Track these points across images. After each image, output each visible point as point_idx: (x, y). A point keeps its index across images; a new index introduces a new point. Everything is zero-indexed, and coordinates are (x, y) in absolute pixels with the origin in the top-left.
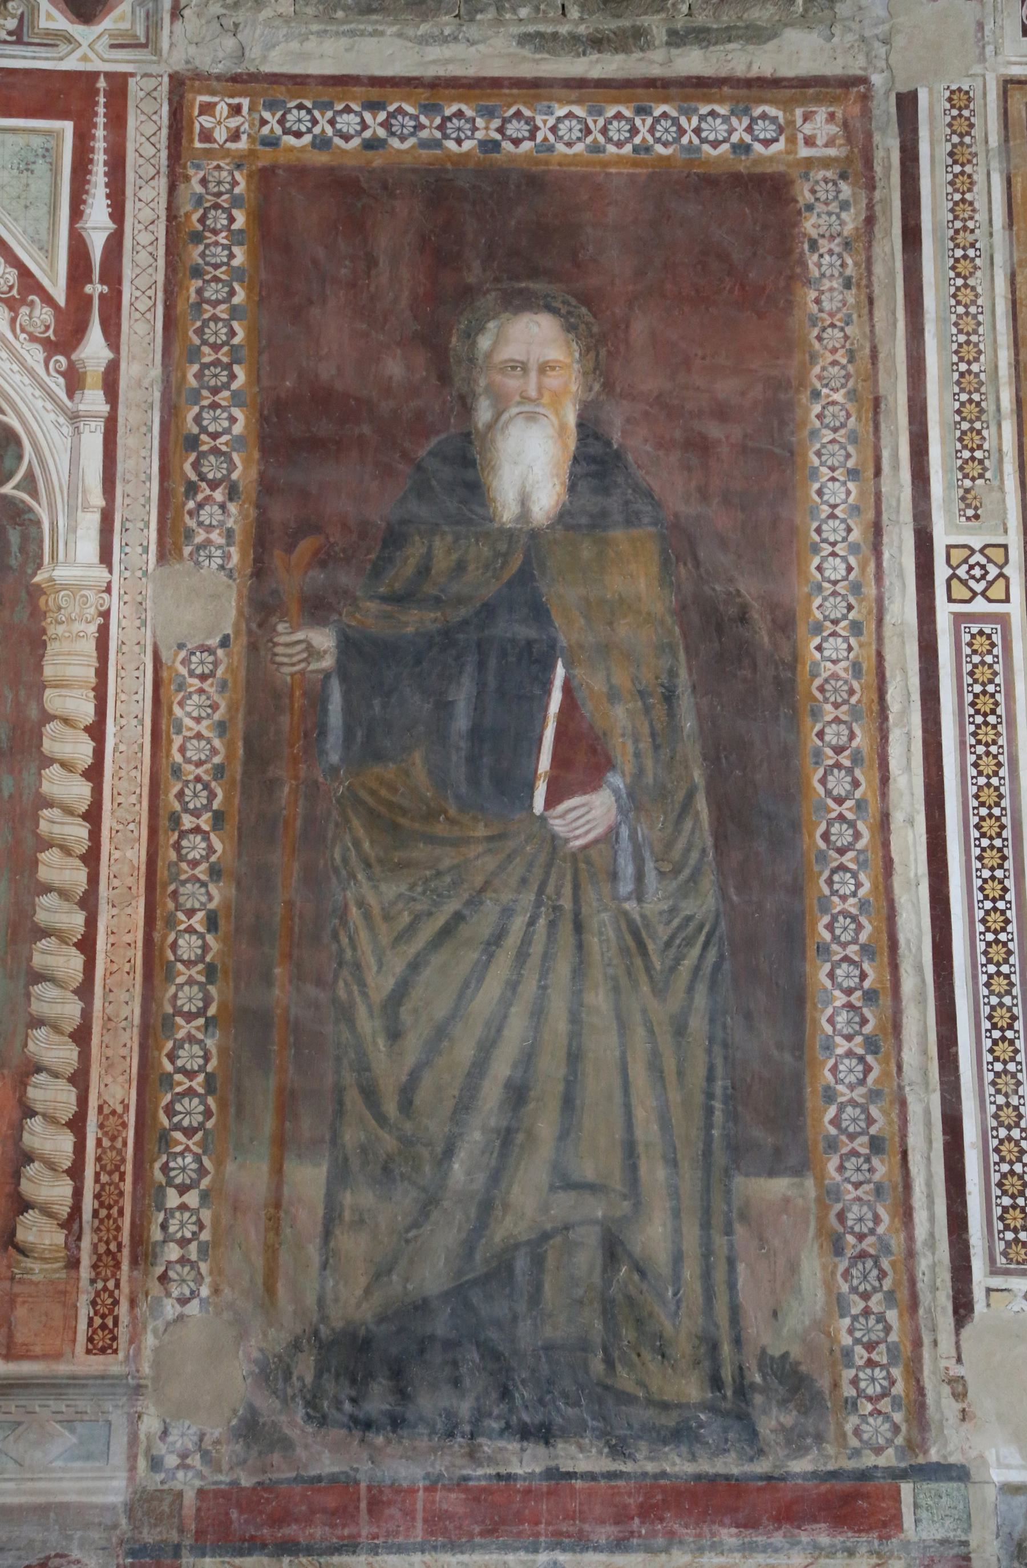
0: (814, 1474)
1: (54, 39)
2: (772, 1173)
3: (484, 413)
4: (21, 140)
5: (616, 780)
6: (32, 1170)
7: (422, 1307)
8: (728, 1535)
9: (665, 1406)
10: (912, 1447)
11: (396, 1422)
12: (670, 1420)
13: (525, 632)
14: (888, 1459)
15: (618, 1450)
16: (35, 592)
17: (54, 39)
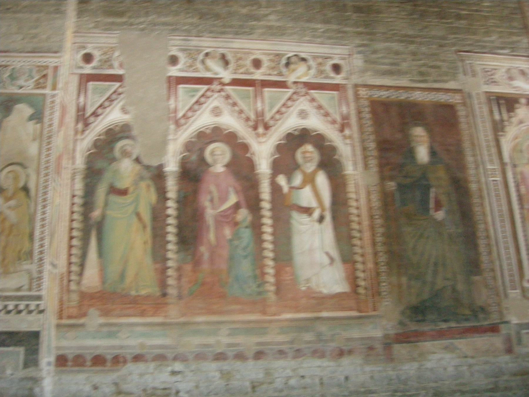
0: (488, 325)
1: (332, 78)
2: (476, 275)
3: (413, 144)
4: (330, 95)
5: (444, 209)
6: (359, 280)
7: (424, 301)
8: (477, 335)
9: (464, 315)
10: (501, 319)
11: (423, 321)
12: (464, 317)
13: (426, 183)
14: (499, 321)
15: (458, 322)
16: (345, 175)
17: (332, 78)
